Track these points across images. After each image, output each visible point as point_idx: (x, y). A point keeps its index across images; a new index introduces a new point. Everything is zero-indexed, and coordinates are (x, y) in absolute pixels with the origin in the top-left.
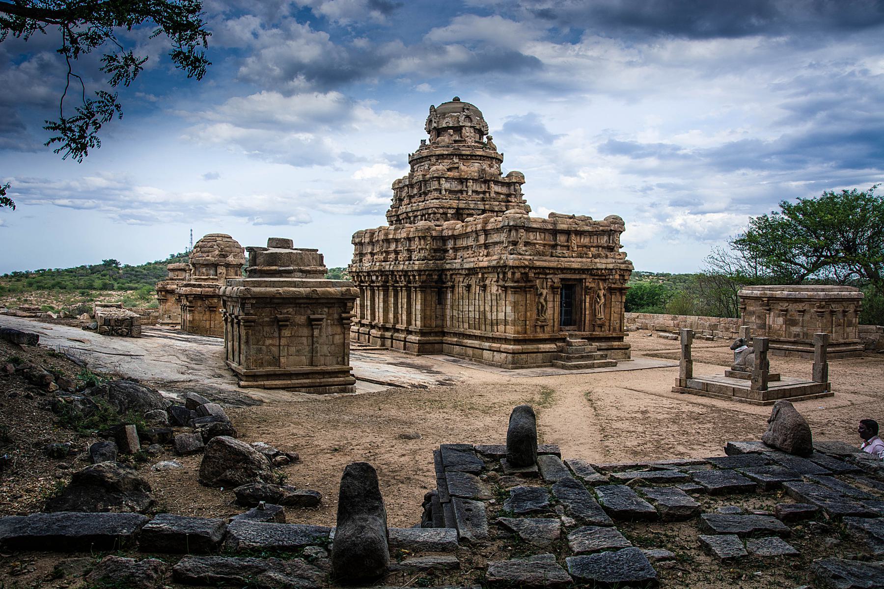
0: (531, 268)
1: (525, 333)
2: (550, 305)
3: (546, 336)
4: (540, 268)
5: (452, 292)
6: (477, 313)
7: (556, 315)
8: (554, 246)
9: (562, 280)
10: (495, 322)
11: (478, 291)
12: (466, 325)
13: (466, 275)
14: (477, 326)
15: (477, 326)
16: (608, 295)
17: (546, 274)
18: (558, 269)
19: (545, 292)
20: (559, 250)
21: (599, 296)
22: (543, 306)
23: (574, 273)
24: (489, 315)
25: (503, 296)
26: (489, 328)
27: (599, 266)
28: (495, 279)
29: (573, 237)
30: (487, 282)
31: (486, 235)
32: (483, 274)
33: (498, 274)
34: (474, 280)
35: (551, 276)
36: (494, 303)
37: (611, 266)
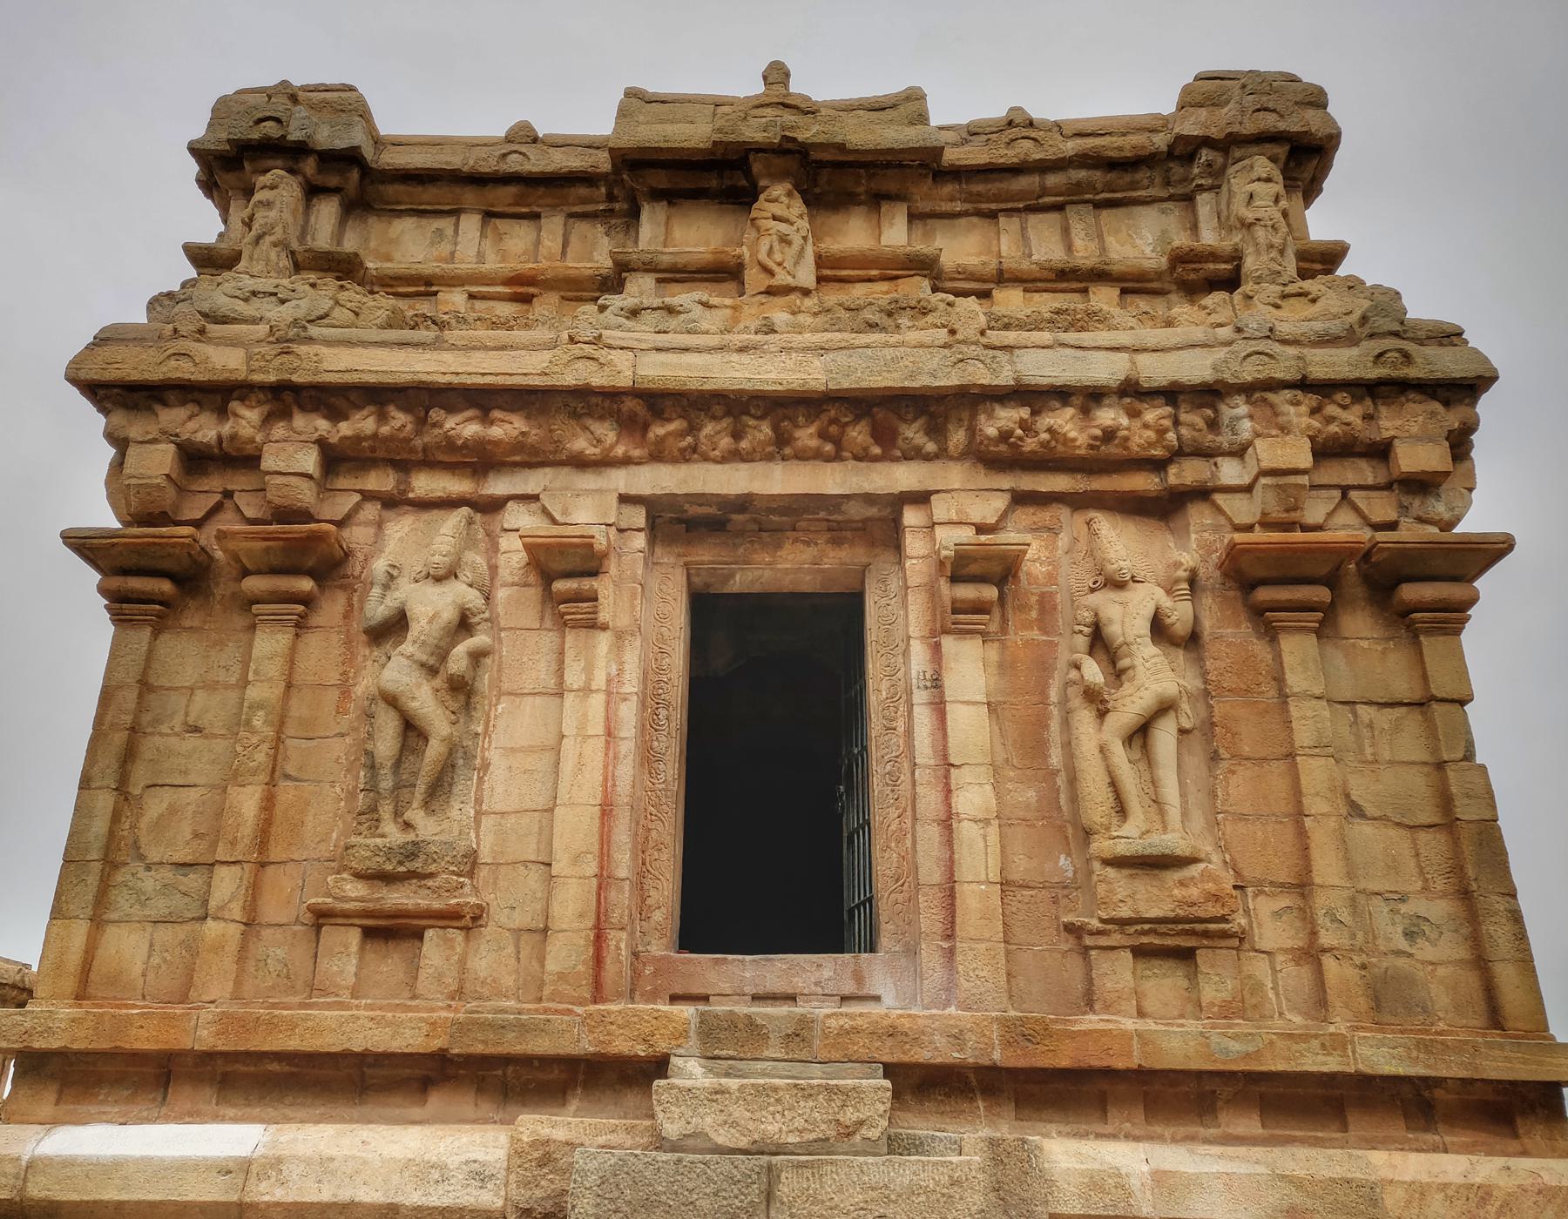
0: (286, 398)
2: (511, 726)
3: (404, 1032)
4: (378, 395)
7: (575, 827)
8: (613, 282)
9: (672, 522)
16: (1229, 633)
17: (482, 460)
18: (586, 402)
19: (431, 607)
20: (640, 288)
21: (1099, 641)
22: (412, 730)
23: (781, 448)
27: (1043, 364)
29: (780, 203)
35: (532, 482)
37: (1195, 368)
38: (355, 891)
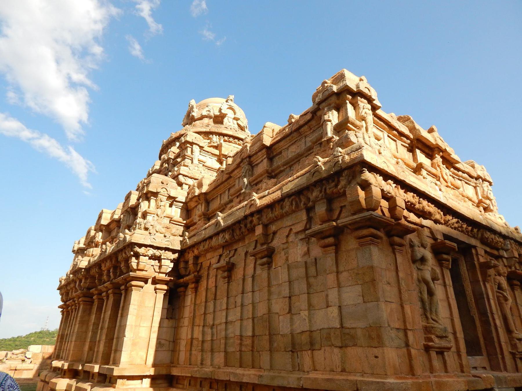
1: (412, 371)
5: (196, 289)
6: (248, 325)
10: (305, 338)
11: (250, 271)
12: (219, 358)
13: (226, 246)
14: (248, 357)
15: (248, 357)
24: (283, 326)
25: (329, 261)
26: (283, 359)
28: (299, 227)
30: (276, 243)
31: (271, 159)
32: (266, 227)
33: (309, 210)
34: (241, 251)
36: (301, 287)
38: (436, 340)
